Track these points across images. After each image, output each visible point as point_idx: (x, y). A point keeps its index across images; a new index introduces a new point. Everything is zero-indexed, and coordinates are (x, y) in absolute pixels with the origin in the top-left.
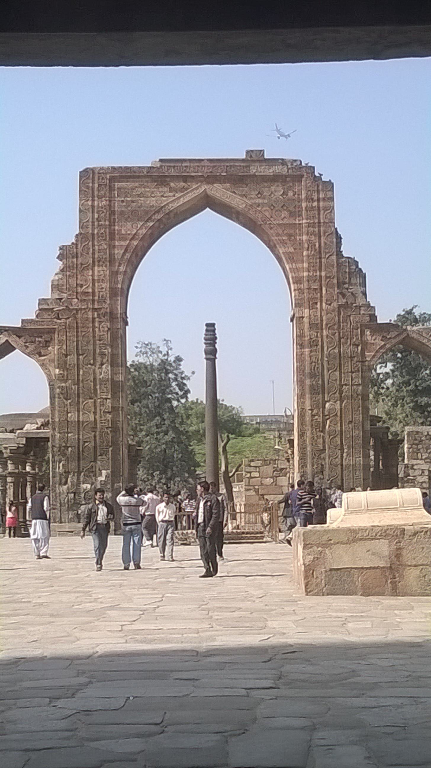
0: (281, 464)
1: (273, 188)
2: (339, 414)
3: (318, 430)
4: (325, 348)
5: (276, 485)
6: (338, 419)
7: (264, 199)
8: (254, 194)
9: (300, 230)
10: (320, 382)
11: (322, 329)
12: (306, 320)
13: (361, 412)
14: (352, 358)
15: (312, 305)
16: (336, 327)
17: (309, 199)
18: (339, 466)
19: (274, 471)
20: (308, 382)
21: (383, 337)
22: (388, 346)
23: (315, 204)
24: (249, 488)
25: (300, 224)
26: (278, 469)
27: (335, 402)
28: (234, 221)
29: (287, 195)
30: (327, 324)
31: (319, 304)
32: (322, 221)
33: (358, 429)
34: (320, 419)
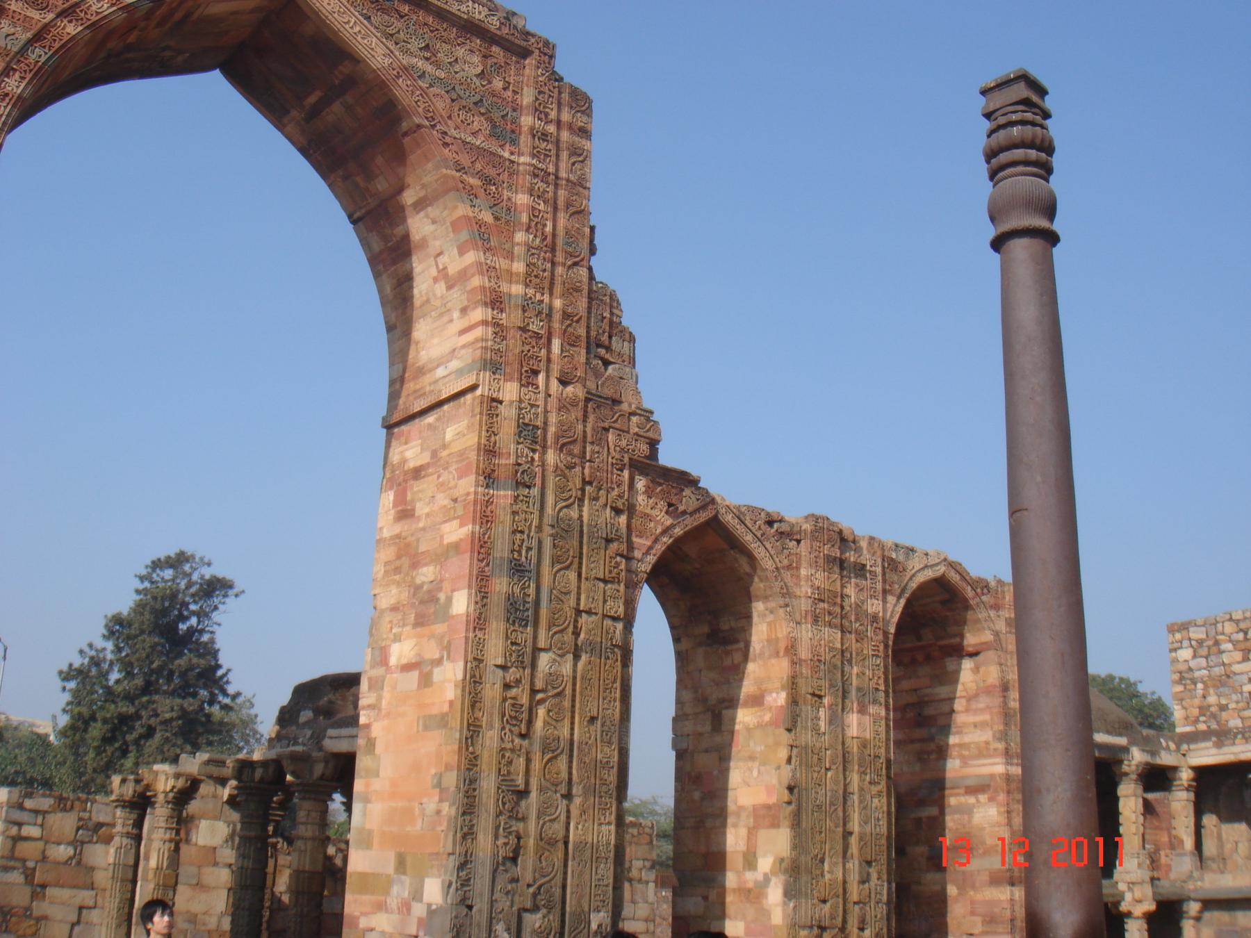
0: (98, 812)
1: (460, 52)
2: (568, 692)
3: (516, 730)
4: (550, 499)
5: (79, 863)
6: (567, 703)
7: (438, 65)
8: (415, 45)
9: (510, 175)
10: (532, 591)
11: (544, 447)
12: (507, 413)
13: (618, 695)
14: (608, 541)
15: (528, 377)
16: (576, 449)
17: (539, 111)
18: (561, 845)
19: (78, 829)
20: (501, 585)
21: (670, 505)
22: (678, 531)
23: (551, 128)
24: (12, 863)
25: (513, 162)
26: (90, 824)
27: (562, 656)
28: (280, 126)
29: (490, 83)
30: (557, 437)
31: (541, 378)
32: (563, 174)
33: (610, 743)
34: (524, 700)
